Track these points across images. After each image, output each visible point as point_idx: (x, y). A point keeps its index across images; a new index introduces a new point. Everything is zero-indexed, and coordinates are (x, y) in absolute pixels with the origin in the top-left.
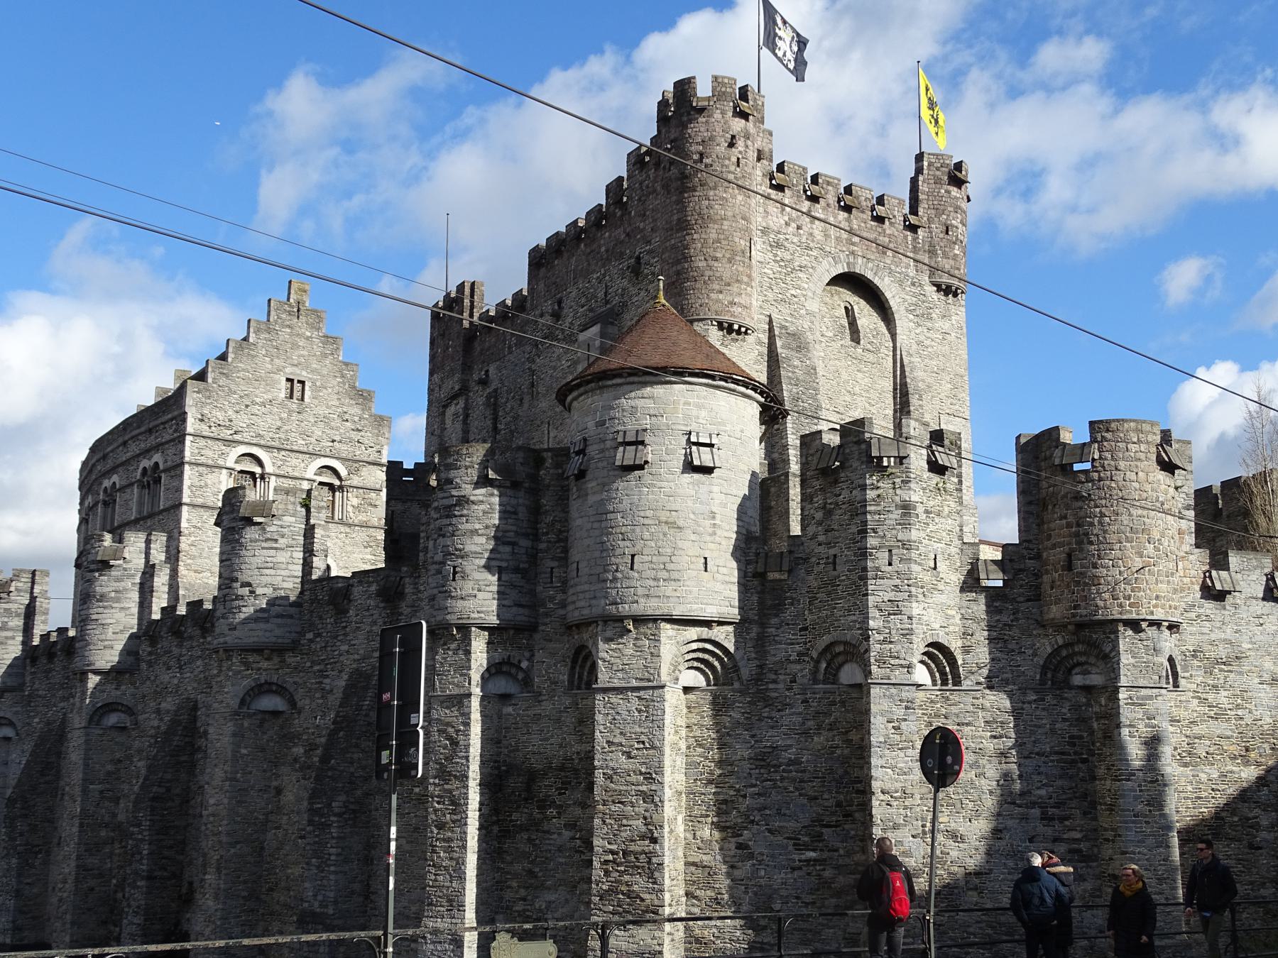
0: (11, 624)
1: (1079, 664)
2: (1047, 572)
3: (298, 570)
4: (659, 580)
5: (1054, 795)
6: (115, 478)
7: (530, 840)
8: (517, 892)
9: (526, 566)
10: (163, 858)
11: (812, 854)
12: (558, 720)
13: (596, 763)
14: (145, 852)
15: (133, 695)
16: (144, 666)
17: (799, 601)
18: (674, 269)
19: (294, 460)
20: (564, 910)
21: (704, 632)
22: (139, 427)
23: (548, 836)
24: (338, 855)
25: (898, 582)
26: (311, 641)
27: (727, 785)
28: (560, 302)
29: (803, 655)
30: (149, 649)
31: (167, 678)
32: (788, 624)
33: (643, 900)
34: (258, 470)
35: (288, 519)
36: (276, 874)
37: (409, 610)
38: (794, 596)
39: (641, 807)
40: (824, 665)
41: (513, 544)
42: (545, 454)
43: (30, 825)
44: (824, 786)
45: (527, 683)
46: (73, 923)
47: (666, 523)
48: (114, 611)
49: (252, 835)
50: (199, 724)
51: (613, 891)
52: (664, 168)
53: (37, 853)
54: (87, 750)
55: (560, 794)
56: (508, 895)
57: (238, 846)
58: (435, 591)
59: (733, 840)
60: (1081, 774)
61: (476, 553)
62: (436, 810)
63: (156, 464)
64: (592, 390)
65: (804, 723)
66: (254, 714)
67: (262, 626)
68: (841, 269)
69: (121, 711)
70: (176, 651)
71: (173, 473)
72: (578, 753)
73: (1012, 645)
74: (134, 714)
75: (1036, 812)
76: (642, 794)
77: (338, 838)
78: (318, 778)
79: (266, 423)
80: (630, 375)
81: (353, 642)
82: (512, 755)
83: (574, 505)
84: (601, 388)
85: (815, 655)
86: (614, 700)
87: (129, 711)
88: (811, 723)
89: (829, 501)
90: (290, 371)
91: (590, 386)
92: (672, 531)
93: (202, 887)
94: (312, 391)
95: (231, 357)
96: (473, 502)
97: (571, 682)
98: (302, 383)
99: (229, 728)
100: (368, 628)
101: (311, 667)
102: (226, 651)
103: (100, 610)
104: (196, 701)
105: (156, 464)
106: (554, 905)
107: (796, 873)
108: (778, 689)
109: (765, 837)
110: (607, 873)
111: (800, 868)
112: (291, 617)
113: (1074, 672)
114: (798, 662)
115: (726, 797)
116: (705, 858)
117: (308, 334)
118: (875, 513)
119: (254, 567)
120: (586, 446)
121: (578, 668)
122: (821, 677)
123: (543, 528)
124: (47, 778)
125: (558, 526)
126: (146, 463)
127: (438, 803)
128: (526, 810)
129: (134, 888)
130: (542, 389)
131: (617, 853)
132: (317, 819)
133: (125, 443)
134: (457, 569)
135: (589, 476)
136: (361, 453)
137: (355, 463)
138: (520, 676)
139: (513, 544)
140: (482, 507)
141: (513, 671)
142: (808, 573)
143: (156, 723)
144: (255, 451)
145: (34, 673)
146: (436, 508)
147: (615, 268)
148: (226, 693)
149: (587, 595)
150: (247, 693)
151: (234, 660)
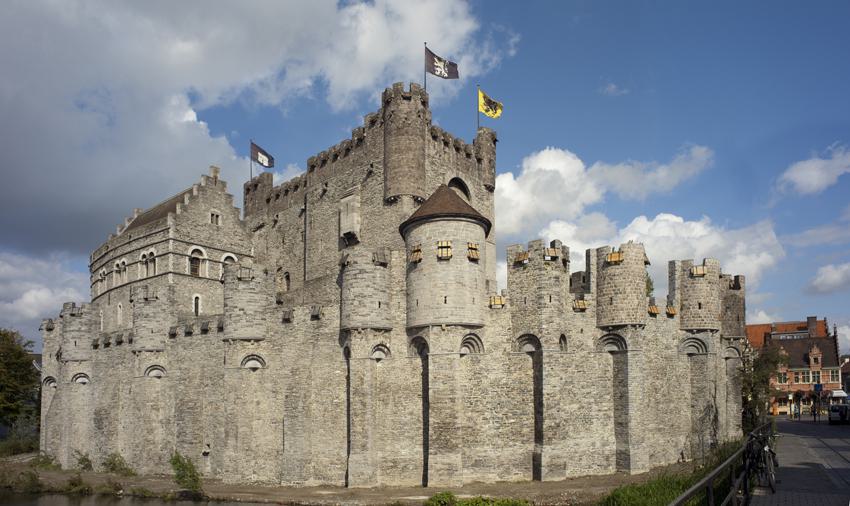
0: (83, 329)
6: (124, 259)
19: (216, 253)
21: (473, 331)
28: (326, 185)
34: (200, 257)
35: (258, 280)
39: (450, 405)
51: (437, 439)
63: (152, 254)
78: (287, 397)
87: (162, 369)
90: (212, 210)
95: (187, 202)
98: (217, 216)
105: (152, 254)
136: (243, 251)
137: (240, 255)
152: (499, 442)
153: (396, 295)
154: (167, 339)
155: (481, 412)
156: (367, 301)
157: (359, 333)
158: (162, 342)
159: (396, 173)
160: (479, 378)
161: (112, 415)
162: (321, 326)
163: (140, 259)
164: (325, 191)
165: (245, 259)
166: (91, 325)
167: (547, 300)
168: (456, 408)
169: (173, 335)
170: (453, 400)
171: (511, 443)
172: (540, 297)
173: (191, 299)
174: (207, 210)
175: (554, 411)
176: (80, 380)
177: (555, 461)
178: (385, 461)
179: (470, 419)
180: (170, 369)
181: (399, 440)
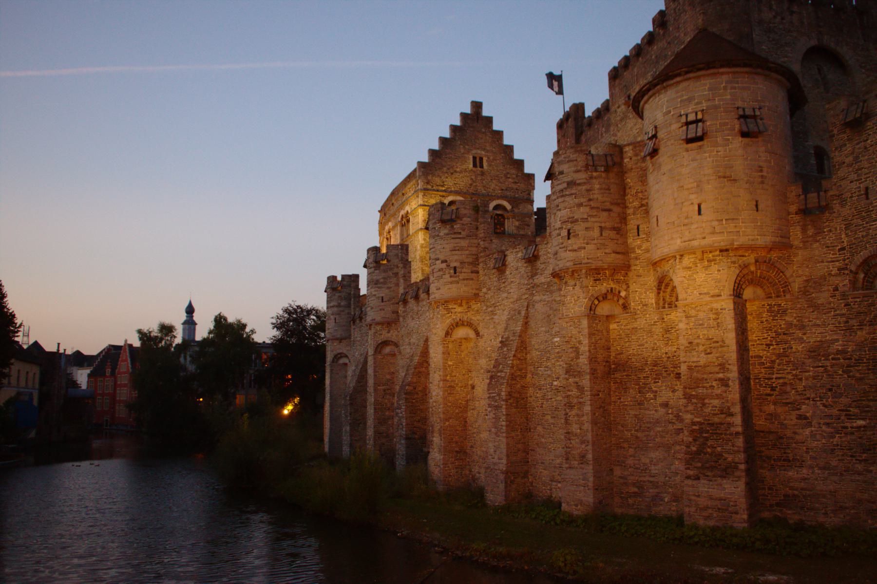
0: (342, 304)
4: (722, 220)
9: (619, 225)
10: (415, 427)
11: (861, 423)
12: (650, 332)
13: (682, 359)
14: (404, 424)
16: (401, 319)
17: (836, 229)
23: (647, 412)
24: (507, 426)
27: (787, 371)
29: (843, 269)
30: (403, 309)
32: (828, 247)
33: (725, 459)
35: (466, 220)
36: (474, 437)
37: (543, 266)
40: (862, 276)
41: (609, 210)
44: (869, 369)
45: (625, 307)
47: (724, 177)
48: (383, 289)
49: (457, 413)
51: (698, 452)
55: (655, 382)
58: (558, 248)
59: (794, 413)
62: (568, 396)
64: (659, 92)
65: (847, 322)
67: (454, 285)
68: (813, 43)
72: (666, 353)
76: (721, 380)
77: (507, 415)
80: (687, 73)
81: (509, 291)
82: (619, 356)
83: (651, 178)
84: (664, 88)
85: (853, 268)
88: (853, 322)
91: (656, 88)
96: (579, 184)
97: (657, 303)
98: (481, 159)
101: (486, 309)
103: (376, 289)
104: (427, 336)
107: (849, 437)
110: (695, 440)
111: (853, 434)
112: (472, 279)
114: (839, 275)
115: (786, 380)
120: (656, 132)
122: (860, 285)
124: (361, 384)
127: (569, 391)
134: (571, 231)
135: (660, 155)
138: (621, 301)
139: (609, 210)
140: (584, 187)
142: (842, 206)
148: (438, 328)
149: (666, 238)
152: (834, 463)
153: (634, 214)
154: (401, 309)
155: (795, 406)
156: (579, 228)
160: (786, 342)
162: (536, 274)
165: (521, 207)
166: (351, 300)
168: (730, 397)
170: (724, 382)
171: (859, 467)
174: (468, 152)
176: (342, 361)
179: (771, 417)
180: (403, 345)
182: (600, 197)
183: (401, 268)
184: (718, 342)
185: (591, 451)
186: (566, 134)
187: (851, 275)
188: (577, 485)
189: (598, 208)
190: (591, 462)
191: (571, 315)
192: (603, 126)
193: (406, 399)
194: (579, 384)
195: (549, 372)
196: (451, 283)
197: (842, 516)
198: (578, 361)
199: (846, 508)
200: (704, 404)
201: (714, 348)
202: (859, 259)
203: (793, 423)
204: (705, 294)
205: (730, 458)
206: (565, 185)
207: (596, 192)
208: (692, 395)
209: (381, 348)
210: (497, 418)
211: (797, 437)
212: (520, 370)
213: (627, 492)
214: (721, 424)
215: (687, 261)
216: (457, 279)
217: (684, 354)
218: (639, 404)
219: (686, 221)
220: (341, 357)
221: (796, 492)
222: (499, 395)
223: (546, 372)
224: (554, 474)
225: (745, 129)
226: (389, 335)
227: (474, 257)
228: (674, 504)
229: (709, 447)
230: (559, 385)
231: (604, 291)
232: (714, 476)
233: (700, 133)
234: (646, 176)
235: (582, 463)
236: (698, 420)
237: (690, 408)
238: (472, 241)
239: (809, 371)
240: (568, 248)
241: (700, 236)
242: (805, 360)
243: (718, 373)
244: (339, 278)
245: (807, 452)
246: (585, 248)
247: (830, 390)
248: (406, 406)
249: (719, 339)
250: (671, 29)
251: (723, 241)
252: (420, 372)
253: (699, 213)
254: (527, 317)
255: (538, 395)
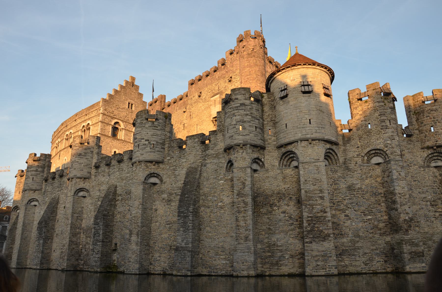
1: (435, 160)
2: (422, 133)
3: (163, 137)
4: (319, 127)
5: (432, 198)
6: (71, 131)
7: (268, 218)
8: (265, 235)
10: (107, 235)
11: (370, 217)
13: (301, 188)
14: (102, 233)
15: (89, 186)
16: (93, 177)
17: (355, 139)
18: (247, 77)
20: (284, 241)
22: (82, 114)
24: (192, 226)
25: (393, 130)
26: (169, 160)
28: (201, 93)
31: (103, 179)
33: (324, 232)
34: (119, 127)
35: (161, 121)
36: (157, 237)
37: (213, 145)
38: (354, 137)
40: (366, 158)
41: (259, 120)
42: (264, 95)
43: (47, 230)
44: (370, 196)
45: (263, 166)
46: (67, 260)
47: (319, 110)
49: (148, 224)
50: (117, 192)
51: (311, 231)
52: (241, 53)
53: (49, 239)
54: (73, 203)
55: (278, 202)
56: (261, 237)
57: (144, 227)
58: (233, 134)
60: (438, 192)
61: (248, 121)
62: (237, 207)
63: (89, 124)
66: (149, 183)
67: (152, 154)
69: (84, 191)
70: (107, 170)
71: (95, 125)
72: (284, 188)
73: (415, 154)
74: (89, 192)
75: (429, 203)
76: (321, 197)
77: (192, 220)
79: (123, 114)
80: (304, 64)
86: (307, 167)
87: (87, 191)
88: (364, 176)
89: (364, 108)
90: (129, 100)
91: (288, 69)
92: (321, 113)
93: (130, 242)
94: (135, 107)
96: (246, 105)
97: (279, 165)
98: (132, 104)
99: (141, 187)
100: (195, 153)
102: (139, 162)
105: (89, 124)
106: (280, 239)
107: (366, 223)
108: (352, 166)
109: (354, 212)
110: (309, 225)
111: (367, 222)
112: (162, 152)
113: (432, 162)
116: (334, 220)
117: (134, 91)
118: (384, 109)
119: (150, 135)
121: (282, 160)
122: (365, 161)
123: (265, 117)
125: (271, 116)
126: (85, 124)
127: (238, 204)
128: (265, 208)
129: (96, 246)
130: (194, 116)
131: (313, 217)
132: (182, 214)
133: (75, 120)
135: (289, 96)
140: (249, 107)
141: (259, 162)
143: (98, 194)
144: (119, 121)
145: (46, 184)
146: (230, 108)
147: (222, 81)
148: (139, 176)
149: (293, 133)
150: (147, 176)
151: (143, 165)
154: (93, 171)
157: (241, 148)
158: (88, 173)
159: (248, 78)
161: (50, 225)
162: (208, 149)
163: (81, 128)
164: (199, 96)
166: (44, 168)
167: (388, 124)
168: (325, 204)
169: (97, 167)
170: (322, 198)
171: (371, 235)
172: (383, 121)
173: (111, 152)
175: (406, 207)
176: (33, 203)
177: (414, 249)
178: (264, 252)
181: (274, 233)
182: (255, 112)
183: (96, 149)
184: (318, 180)
185: (252, 234)
186: (154, 109)
187: (362, 158)
188: (243, 252)
189: (254, 117)
190: (252, 240)
191: (240, 167)
192: (177, 106)
193: (104, 218)
194: (245, 201)
195: (215, 199)
196: (151, 152)
197: (366, 257)
198: (244, 189)
199: (367, 253)
200: (313, 208)
201: (317, 182)
202: (366, 151)
203: (343, 218)
204: (312, 159)
205: (326, 232)
206: (239, 105)
207: (254, 110)
208: (307, 204)
209: (78, 192)
210: (185, 223)
211: (346, 224)
212: (198, 197)
213: (265, 256)
214: (321, 217)
215: (304, 143)
216: (154, 150)
217: (303, 185)
218: (270, 213)
219: (304, 126)
220: (33, 201)
221: (347, 248)
222: (187, 209)
223: (213, 199)
224: (218, 251)
225: (327, 92)
226: (84, 185)
227: (163, 141)
228: (291, 259)
229: (316, 228)
230: (222, 205)
231: (256, 157)
232: (319, 241)
233: (310, 90)
234: (275, 107)
235: (246, 241)
236: (310, 215)
237: (307, 210)
238: (163, 132)
239: (348, 196)
240: (240, 134)
241: (311, 133)
242: (347, 192)
243: (319, 194)
244: (38, 155)
245: (350, 231)
246: (249, 135)
247: (357, 204)
248: (103, 222)
249: (319, 179)
250: (228, 66)
251: (320, 136)
252: (111, 204)
253: (310, 123)
254: (201, 171)
255: (207, 211)
